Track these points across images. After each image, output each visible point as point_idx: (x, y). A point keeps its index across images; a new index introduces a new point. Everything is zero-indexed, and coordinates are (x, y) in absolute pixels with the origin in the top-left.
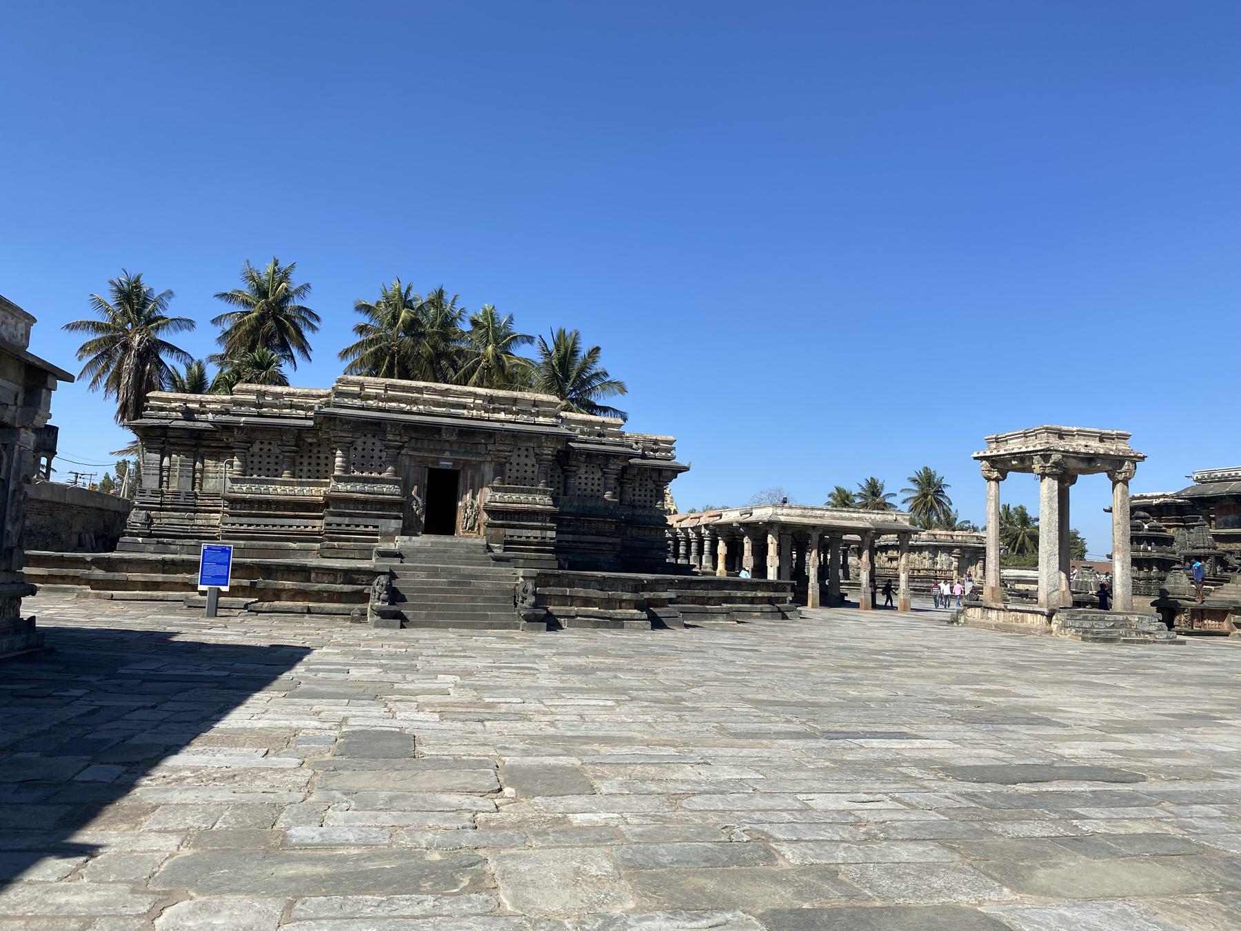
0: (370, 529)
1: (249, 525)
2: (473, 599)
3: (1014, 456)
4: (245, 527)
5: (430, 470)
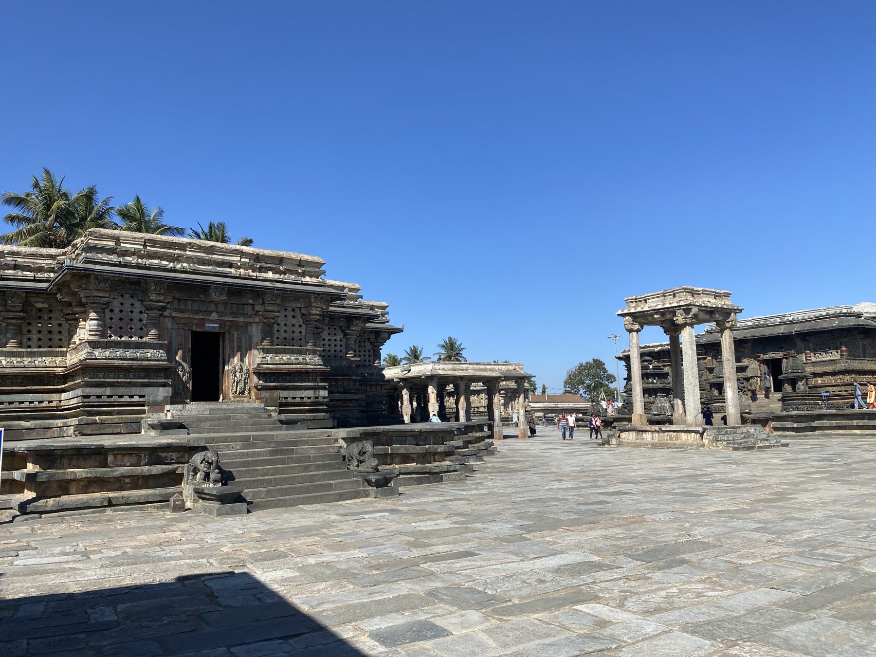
1: (10, 403)
2: (306, 469)
3: (657, 311)
5: (194, 334)
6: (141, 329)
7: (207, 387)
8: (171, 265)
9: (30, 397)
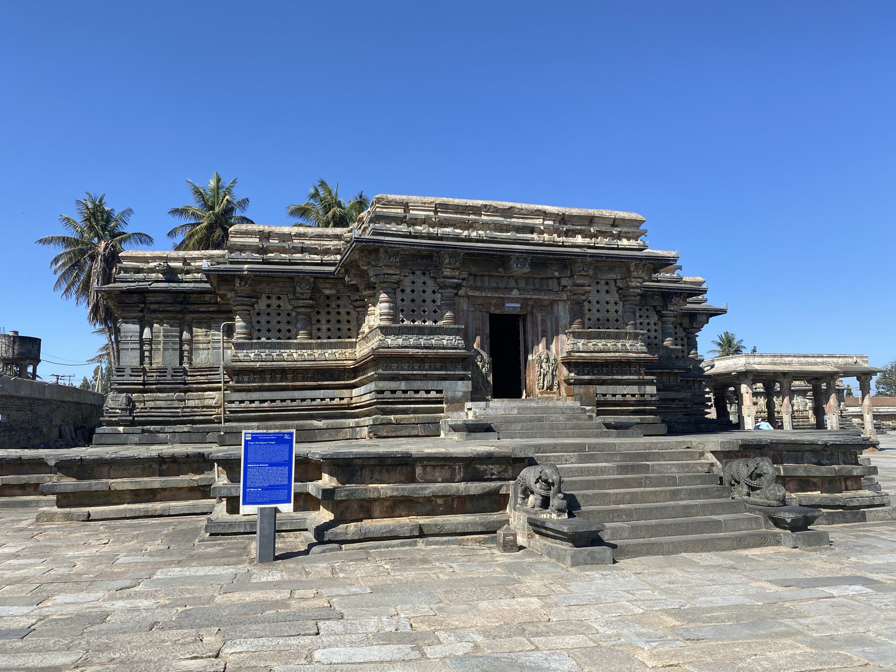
0: (433, 394)
2: (674, 495)
4: (257, 404)
5: (493, 317)
6: (435, 312)
7: (508, 382)
8: (466, 233)
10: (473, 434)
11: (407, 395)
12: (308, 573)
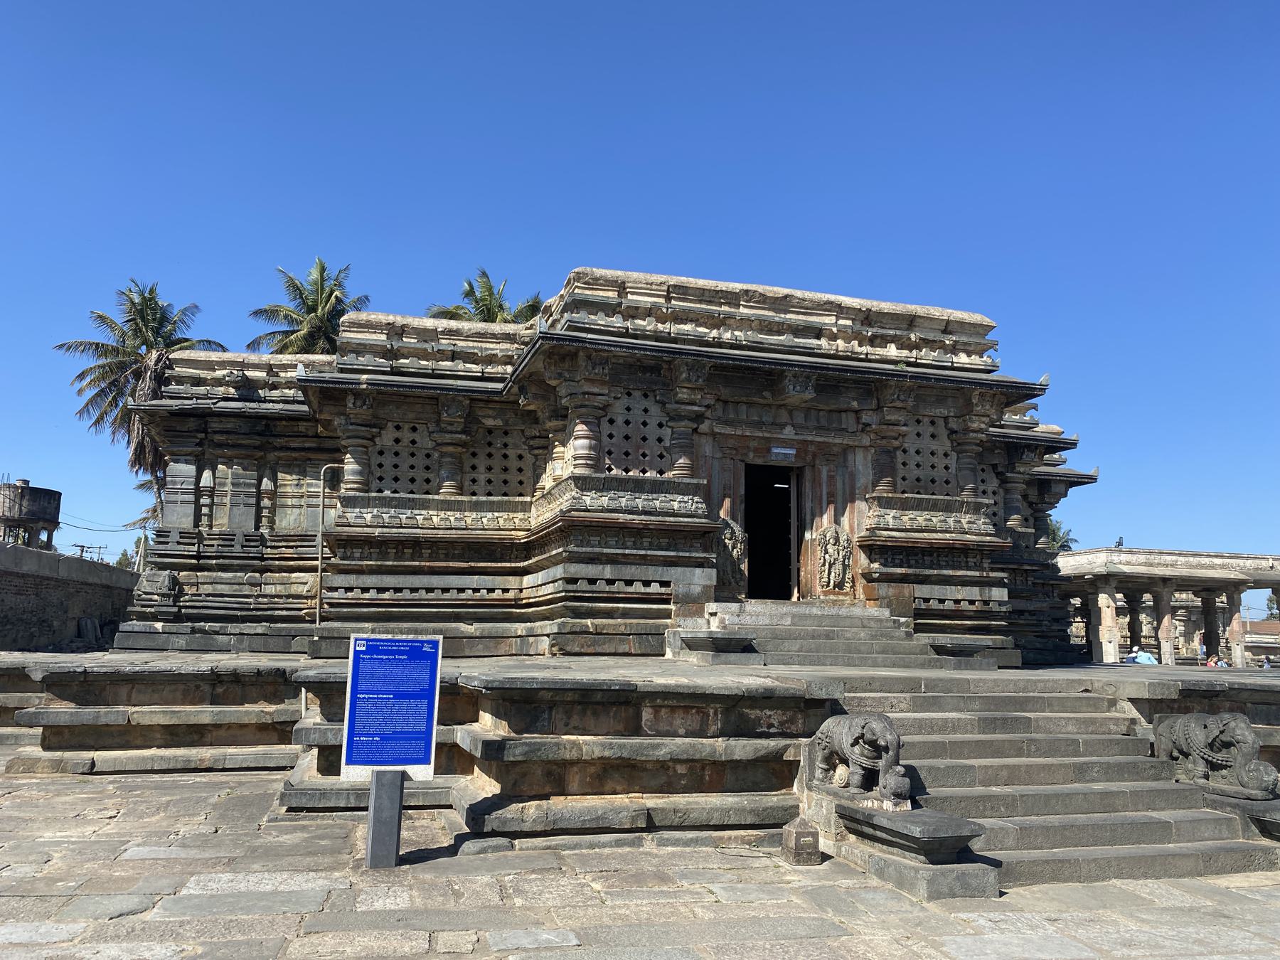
0: (655, 588)
2: (1081, 772)
4: (372, 594)
5: (751, 470)
6: (661, 456)
7: (772, 574)
8: (714, 333)
9: (474, 581)
10: (724, 656)
11: (614, 588)
12: (458, 895)
